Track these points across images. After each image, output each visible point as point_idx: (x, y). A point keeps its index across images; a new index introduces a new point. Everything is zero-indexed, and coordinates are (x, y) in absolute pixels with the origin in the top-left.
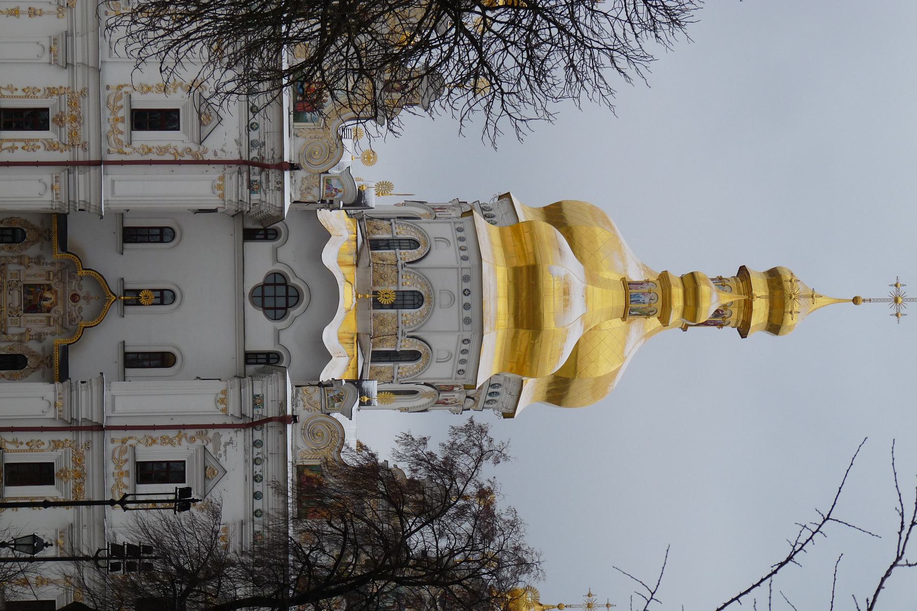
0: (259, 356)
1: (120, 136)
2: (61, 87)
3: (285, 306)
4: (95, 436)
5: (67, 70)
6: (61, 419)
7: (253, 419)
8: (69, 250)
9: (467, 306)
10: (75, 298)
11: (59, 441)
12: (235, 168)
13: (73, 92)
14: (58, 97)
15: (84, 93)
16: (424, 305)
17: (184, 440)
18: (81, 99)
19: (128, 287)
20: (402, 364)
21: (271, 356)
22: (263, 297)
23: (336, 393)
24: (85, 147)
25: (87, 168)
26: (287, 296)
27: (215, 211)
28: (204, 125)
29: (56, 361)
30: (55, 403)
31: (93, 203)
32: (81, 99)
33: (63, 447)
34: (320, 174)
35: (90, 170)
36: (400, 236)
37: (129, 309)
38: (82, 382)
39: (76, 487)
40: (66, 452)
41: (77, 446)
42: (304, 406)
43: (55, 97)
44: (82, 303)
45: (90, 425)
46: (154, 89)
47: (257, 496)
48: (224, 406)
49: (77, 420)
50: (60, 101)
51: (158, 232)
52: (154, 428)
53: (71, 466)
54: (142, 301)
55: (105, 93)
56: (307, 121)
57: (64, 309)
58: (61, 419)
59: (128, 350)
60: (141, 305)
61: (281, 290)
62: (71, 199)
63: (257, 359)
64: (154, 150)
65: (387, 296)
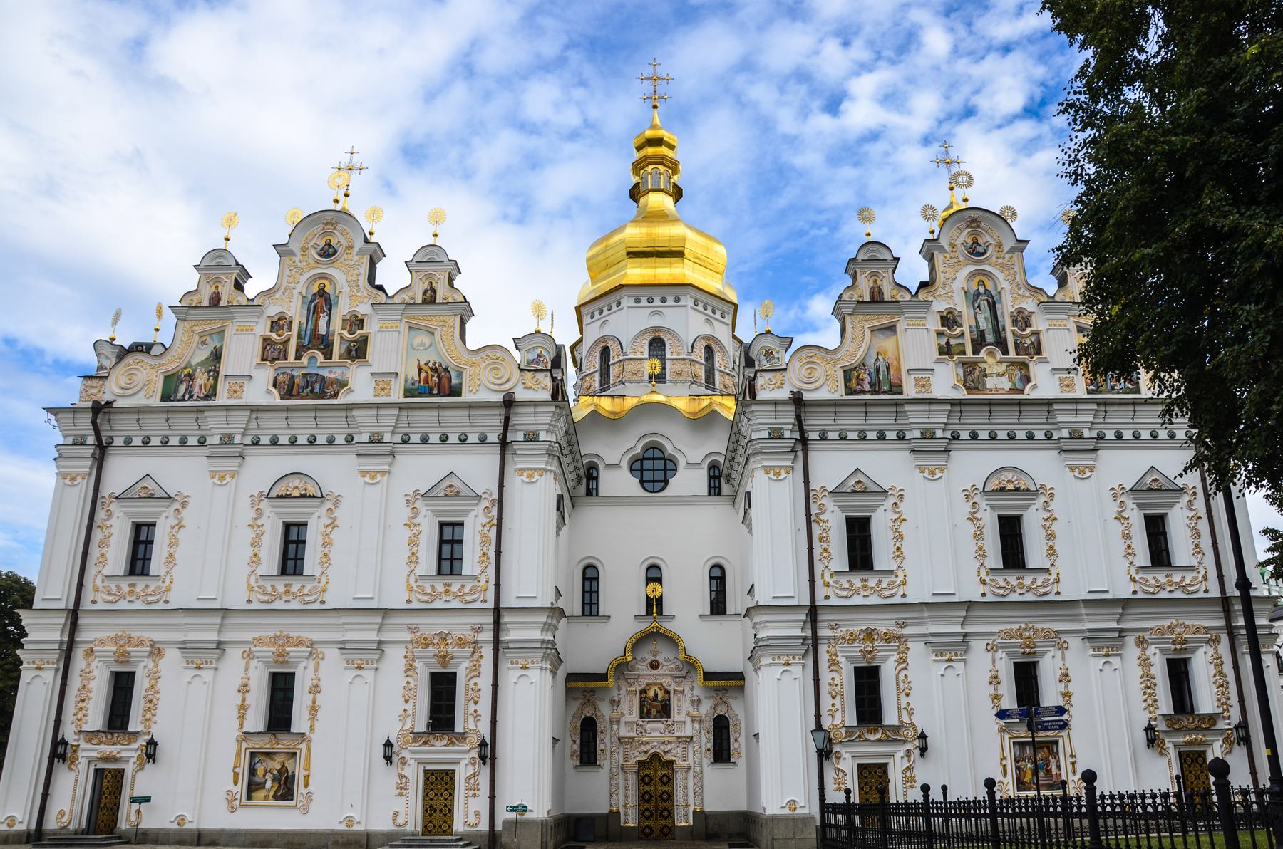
0: (712, 485)
2: (406, 657)
3: (663, 461)
4: (823, 617)
6: (804, 656)
7: (796, 439)
8: (604, 672)
9: (664, 300)
10: (654, 665)
11: (829, 660)
12: (508, 457)
13: (412, 642)
14: (417, 660)
16: (663, 337)
17: (821, 517)
18: (419, 634)
19: (644, 613)
20: (717, 365)
21: (712, 474)
22: (654, 481)
23: (762, 357)
25: (502, 626)
26: (654, 459)
27: (560, 499)
29: (722, 683)
30: (784, 664)
31: (544, 619)
33: (837, 656)
34: (521, 370)
35: (506, 623)
36: (598, 366)
37: (666, 612)
38: (755, 635)
39: (882, 639)
40: (841, 652)
41: (834, 638)
42: (779, 388)
43: (416, 664)
44: (660, 658)
47: (881, 437)
48: (783, 471)
49: (805, 639)
51: (587, 583)
52: (811, 549)
54: (658, 595)
55: (415, 605)
56: (461, 384)
57: (666, 676)
58: (804, 656)
59: (708, 612)
60: (661, 596)
61: (648, 465)
62: (538, 645)
63: (715, 487)
64: (485, 550)
65: (654, 366)
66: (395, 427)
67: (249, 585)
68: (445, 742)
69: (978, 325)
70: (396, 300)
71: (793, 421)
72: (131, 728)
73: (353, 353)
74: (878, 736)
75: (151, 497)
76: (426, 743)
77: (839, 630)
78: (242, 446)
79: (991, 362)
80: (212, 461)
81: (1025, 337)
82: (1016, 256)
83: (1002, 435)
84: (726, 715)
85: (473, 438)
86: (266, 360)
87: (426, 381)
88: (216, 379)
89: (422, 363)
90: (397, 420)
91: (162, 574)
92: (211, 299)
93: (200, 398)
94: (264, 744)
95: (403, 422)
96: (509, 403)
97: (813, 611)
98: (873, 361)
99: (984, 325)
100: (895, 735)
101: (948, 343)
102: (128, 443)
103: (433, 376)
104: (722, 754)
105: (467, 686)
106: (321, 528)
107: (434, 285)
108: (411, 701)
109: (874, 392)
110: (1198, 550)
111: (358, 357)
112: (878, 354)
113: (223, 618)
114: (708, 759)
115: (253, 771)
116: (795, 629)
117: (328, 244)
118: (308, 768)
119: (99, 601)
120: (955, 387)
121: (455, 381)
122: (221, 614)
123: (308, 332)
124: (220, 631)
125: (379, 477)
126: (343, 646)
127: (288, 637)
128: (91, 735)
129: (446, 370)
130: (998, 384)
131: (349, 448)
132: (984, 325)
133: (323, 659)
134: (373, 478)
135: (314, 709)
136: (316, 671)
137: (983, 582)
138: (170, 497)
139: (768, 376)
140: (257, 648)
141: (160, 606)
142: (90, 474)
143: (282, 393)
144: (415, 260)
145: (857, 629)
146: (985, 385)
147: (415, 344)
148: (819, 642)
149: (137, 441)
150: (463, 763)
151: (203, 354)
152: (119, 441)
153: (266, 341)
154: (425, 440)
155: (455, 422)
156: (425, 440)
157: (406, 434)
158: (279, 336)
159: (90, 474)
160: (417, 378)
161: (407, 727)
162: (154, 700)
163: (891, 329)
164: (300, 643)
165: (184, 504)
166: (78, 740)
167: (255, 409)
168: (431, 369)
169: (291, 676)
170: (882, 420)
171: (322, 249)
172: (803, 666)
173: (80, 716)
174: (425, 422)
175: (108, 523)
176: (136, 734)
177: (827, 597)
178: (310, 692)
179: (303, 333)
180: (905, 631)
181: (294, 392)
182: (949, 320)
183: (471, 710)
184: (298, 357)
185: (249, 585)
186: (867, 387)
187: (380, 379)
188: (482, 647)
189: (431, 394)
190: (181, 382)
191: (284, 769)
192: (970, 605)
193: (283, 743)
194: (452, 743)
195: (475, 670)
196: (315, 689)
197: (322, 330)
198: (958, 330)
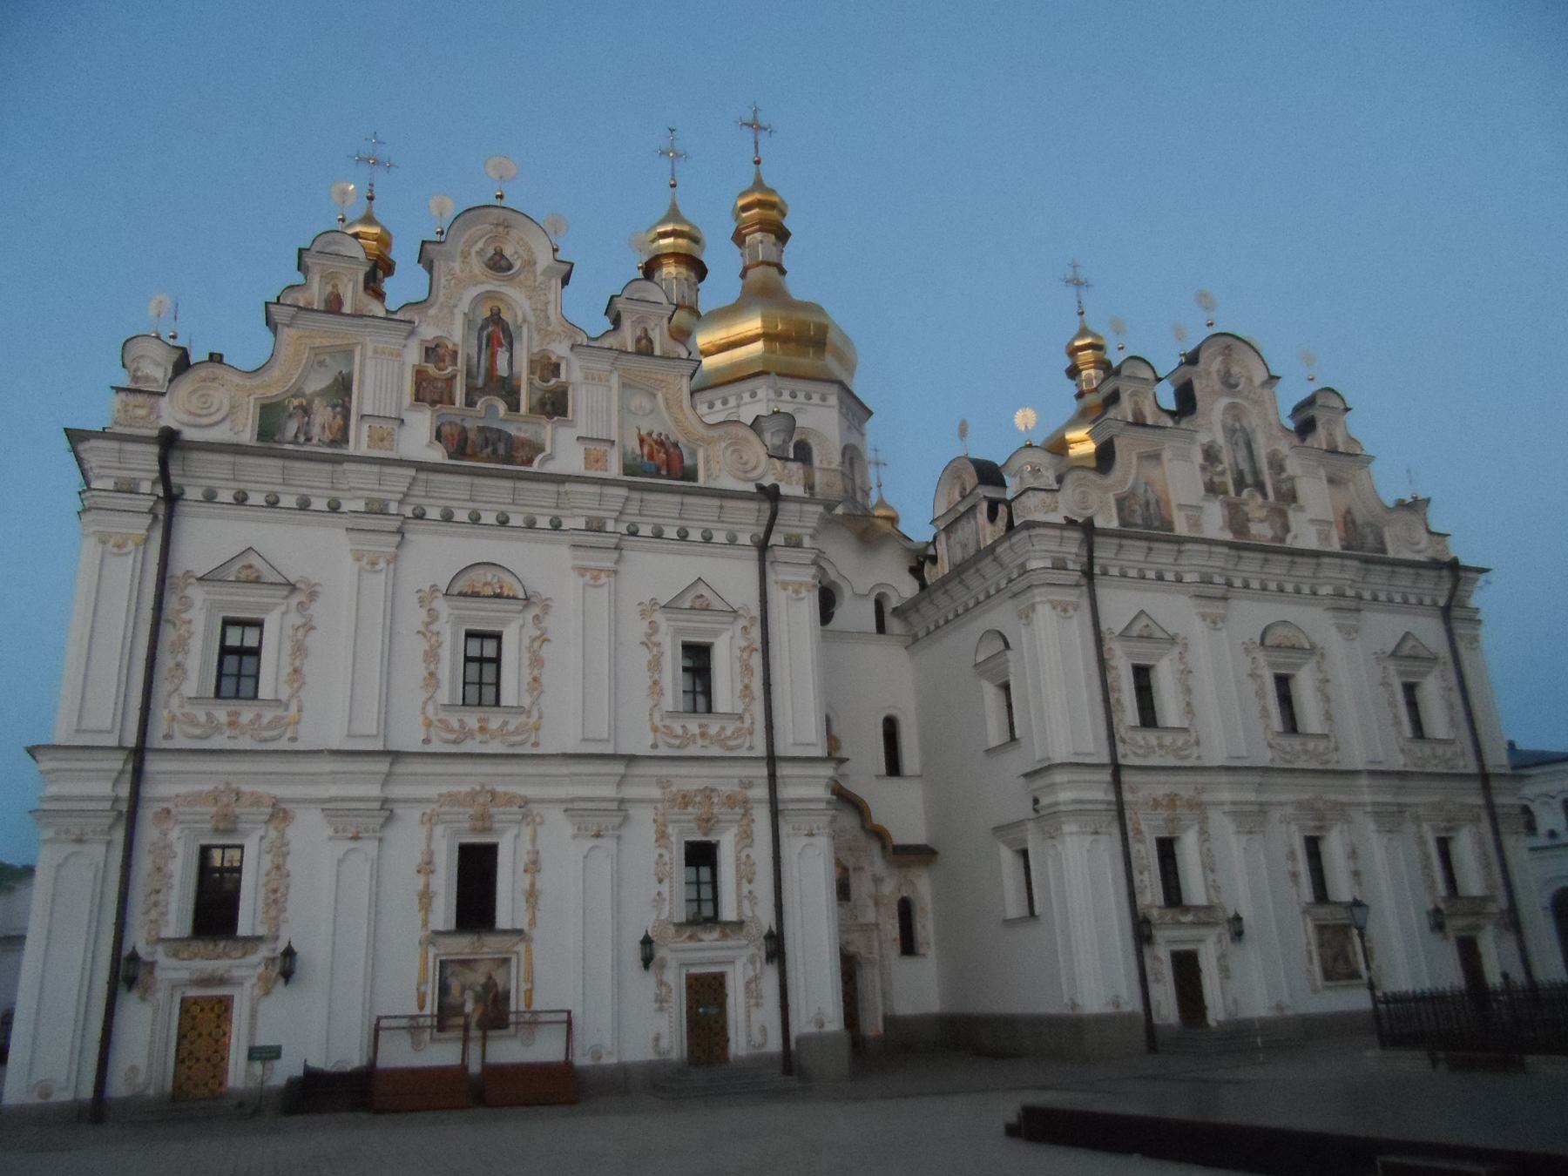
1: (729, 732)
2: (655, 821)
4: (1127, 778)
5: (631, 812)
9: (809, 397)
13: (663, 801)
15: (663, 783)
24: (747, 784)
25: (779, 781)
28: (708, 605)
32: (674, 789)
35: (783, 777)
38: (1036, 801)
45: (1111, 788)
46: (656, 676)
49: (1109, 803)
50: (675, 822)
53: (1163, 813)
55: (663, 751)
64: (746, 681)
66: (621, 513)
67: (426, 718)
68: (716, 934)
69: (1237, 465)
70: (607, 343)
71: (1075, 550)
72: (244, 927)
73: (548, 407)
74: (1189, 918)
75: (257, 581)
76: (691, 938)
77: (1140, 794)
78: (402, 518)
79: (1254, 505)
80: (354, 535)
81: (1283, 481)
82: (1266, 392)
83: (1273, 586)
84: (912, 896)
85: (719, 537)
86: (423, 401)
87: (651, 457)
88: (346, 417)
89: (644, 432)
90: (624, 504)
91: (284, 693)
92: (327, 301)
93: (324, 443)
94: (463, 945)
95: (633, 508)
96: (771, 495)
97: (1117, 769)
98: (1142, 491)
99: (1244, 466)
100: (1207, 916)
101: (1211, 480)
102: (210, 497)
103: (659, 452)
104: (908, 945)
105: (738, 859)
106: (526, 642)
107: (650, 332)
108: (666, 882)
109: (1148, 527)
110: (1453, 723)
111: (556, 414)
112: (1146, 484)
113: (392, 764)
114: (894, 950)
115: (444, 989)
116: (1097, 791)
117: (499, 254)
118: (530, 979)
119: (177, 734)
120: (1221, 529)
121: (687, 462)
122: (389, 759)
123: (482, 371)
124: (385, 783)
125: (603, 579)
126: (572, 808)
127: (493, 794)
128: (176, 946)
129: (676, 445)
130: (1261, 531)
131: (556, 536)
132: (1244, 466)
133: (541, 823)
134: (595, 578)
135: (532, 895)
136: (534, 840)
137: (1270, 746)
138: (289, 584)
139: (1042, 495)
140: (443, 809)
141: (283, 744)
142: (147, 540)
143: (451, 449)
144: (626, 294)
145: (1161, 793)
146: (1247, 528)
147: (633, 409)
148: (1125, 807)
149: (226, 496)
150: (739, 966)
151: (319, 382)
152: (193, 493)
153: (420, 376)
154: (658, 535)
155: (702, 512)
156: (658, 535)
157: (633, 524)
158: (440, 369)
159: (147, 540)
160: (638, 451)
161: (665, 915)
162: (282, 890)
163: (1155, 457)
164: (510, 800)
165: (313, 596)
166: (152, 954)
167: (421, 466)
168: (656, 442)
169: (490, 851)
170: (1163, 556)
171: (491, 259)
172: (1110, 835)
173: (153, 915)
174: (664, 508)
175: (185, 616)
176: (258, 939)
177: (1125, 756)
178: (526, 871)
179: (475, 370)
180: (1206, 797)
181: (469, 451)
182: (1211, 455)
183: (745, 891)
184: (470, 403)
185: (426, 718)
186: (1139, 521)
187: (591, 446)
188: (752, 808)
189: (658, 475)
190: (290, 416)
191: (490, 985)
192: (1266, 770)
193: (490, 945)
194: (724, 936)
195: (746, 837)
196: (534, 866)
197: (502, 369)
198: (1220, 468)
